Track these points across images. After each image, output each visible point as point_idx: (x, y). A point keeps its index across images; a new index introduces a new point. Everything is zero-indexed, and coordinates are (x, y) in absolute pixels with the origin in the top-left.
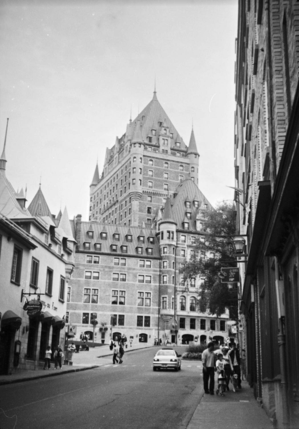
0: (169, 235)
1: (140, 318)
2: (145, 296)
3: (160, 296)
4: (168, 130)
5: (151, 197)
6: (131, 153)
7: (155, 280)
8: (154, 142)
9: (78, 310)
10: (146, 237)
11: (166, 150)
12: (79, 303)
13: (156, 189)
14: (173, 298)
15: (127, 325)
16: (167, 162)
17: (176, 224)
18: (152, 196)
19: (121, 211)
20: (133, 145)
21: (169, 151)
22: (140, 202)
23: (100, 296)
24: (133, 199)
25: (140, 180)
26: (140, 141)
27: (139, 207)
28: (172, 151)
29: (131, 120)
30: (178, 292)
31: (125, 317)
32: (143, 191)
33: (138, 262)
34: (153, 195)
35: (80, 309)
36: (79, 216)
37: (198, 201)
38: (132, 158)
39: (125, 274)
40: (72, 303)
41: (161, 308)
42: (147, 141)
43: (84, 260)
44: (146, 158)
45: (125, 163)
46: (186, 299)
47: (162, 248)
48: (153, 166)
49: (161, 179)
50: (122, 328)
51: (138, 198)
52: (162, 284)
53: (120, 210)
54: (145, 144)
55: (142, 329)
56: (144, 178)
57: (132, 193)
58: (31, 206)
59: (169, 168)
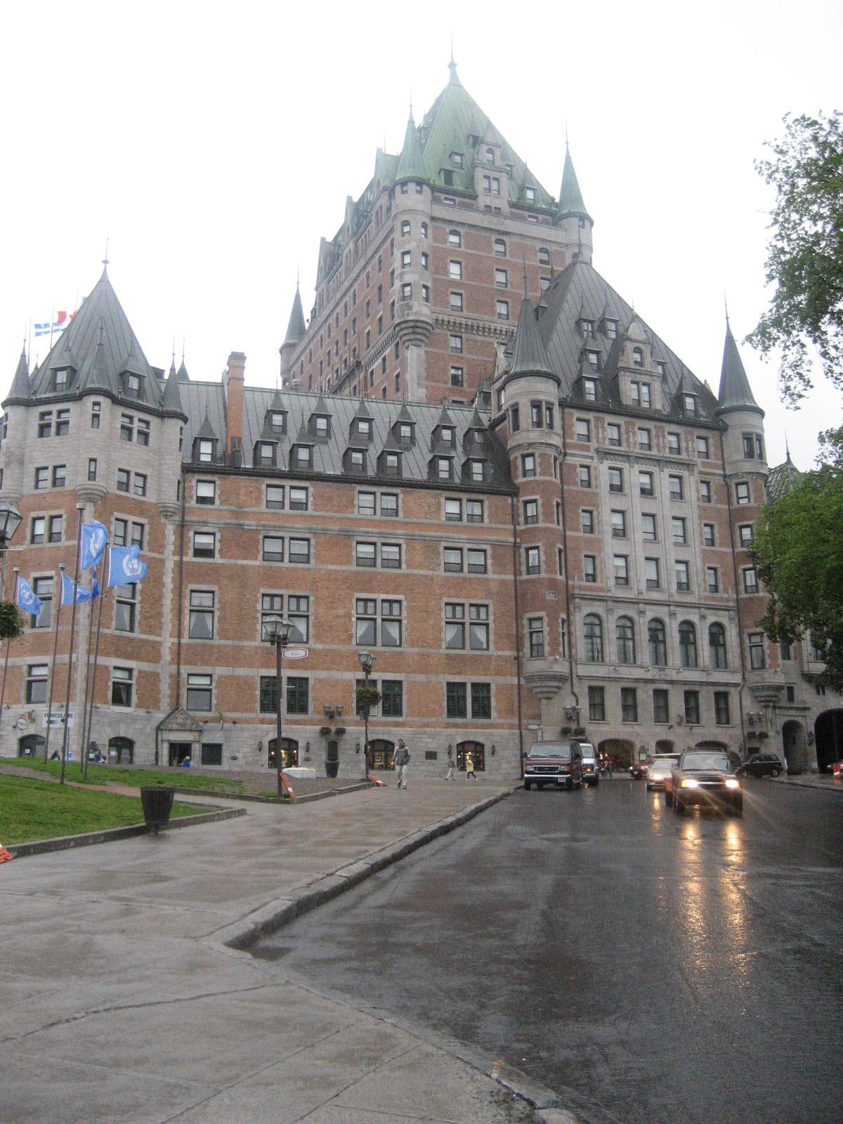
0: (539, 414)
1: (455, 690)
2: (470, 615)
3: (518, 617)
4: (498, 152)
5: (461, 337)
6: (393, 212)
8: (458, 185)
9: (241, 667)
10: (460, 434)
11: (495, 208)
12: (246, 643)
13: (475, 316)
14: (563, 621)
15: (411, 714)
16: (501, 237)
17: (559, 385)
18: (463, 335)
19: (369, 390)
20: (398, 189)
21: (506, 209)
22: (426, 352)
23: (316, 618)
24: (406, 344)
25: (425, 287)
26: (420, 174)
28: (514, 210)
30: (577, 601)
31: (405, 685)
32: (437, 320)
33: (439, 504)
34: (466, 332)
35: (251, 665)
36: (237, 360)
39: (399, 546)
40: (223, 642)
41: (523, 657)
42: (440, 182)
43: (259, 499)
44: (440, 225)
45: (376, 252)
46: (605, 625)
47: (516, 458)
48: (463, 249)
50: (397, 724)
51: (422, 341)
52: (525, 577)
53: (366, 389)
54: (434, 189)
55: (465, 726)
56: (435, 280)
57: (403, 326)
59: (508, 255)
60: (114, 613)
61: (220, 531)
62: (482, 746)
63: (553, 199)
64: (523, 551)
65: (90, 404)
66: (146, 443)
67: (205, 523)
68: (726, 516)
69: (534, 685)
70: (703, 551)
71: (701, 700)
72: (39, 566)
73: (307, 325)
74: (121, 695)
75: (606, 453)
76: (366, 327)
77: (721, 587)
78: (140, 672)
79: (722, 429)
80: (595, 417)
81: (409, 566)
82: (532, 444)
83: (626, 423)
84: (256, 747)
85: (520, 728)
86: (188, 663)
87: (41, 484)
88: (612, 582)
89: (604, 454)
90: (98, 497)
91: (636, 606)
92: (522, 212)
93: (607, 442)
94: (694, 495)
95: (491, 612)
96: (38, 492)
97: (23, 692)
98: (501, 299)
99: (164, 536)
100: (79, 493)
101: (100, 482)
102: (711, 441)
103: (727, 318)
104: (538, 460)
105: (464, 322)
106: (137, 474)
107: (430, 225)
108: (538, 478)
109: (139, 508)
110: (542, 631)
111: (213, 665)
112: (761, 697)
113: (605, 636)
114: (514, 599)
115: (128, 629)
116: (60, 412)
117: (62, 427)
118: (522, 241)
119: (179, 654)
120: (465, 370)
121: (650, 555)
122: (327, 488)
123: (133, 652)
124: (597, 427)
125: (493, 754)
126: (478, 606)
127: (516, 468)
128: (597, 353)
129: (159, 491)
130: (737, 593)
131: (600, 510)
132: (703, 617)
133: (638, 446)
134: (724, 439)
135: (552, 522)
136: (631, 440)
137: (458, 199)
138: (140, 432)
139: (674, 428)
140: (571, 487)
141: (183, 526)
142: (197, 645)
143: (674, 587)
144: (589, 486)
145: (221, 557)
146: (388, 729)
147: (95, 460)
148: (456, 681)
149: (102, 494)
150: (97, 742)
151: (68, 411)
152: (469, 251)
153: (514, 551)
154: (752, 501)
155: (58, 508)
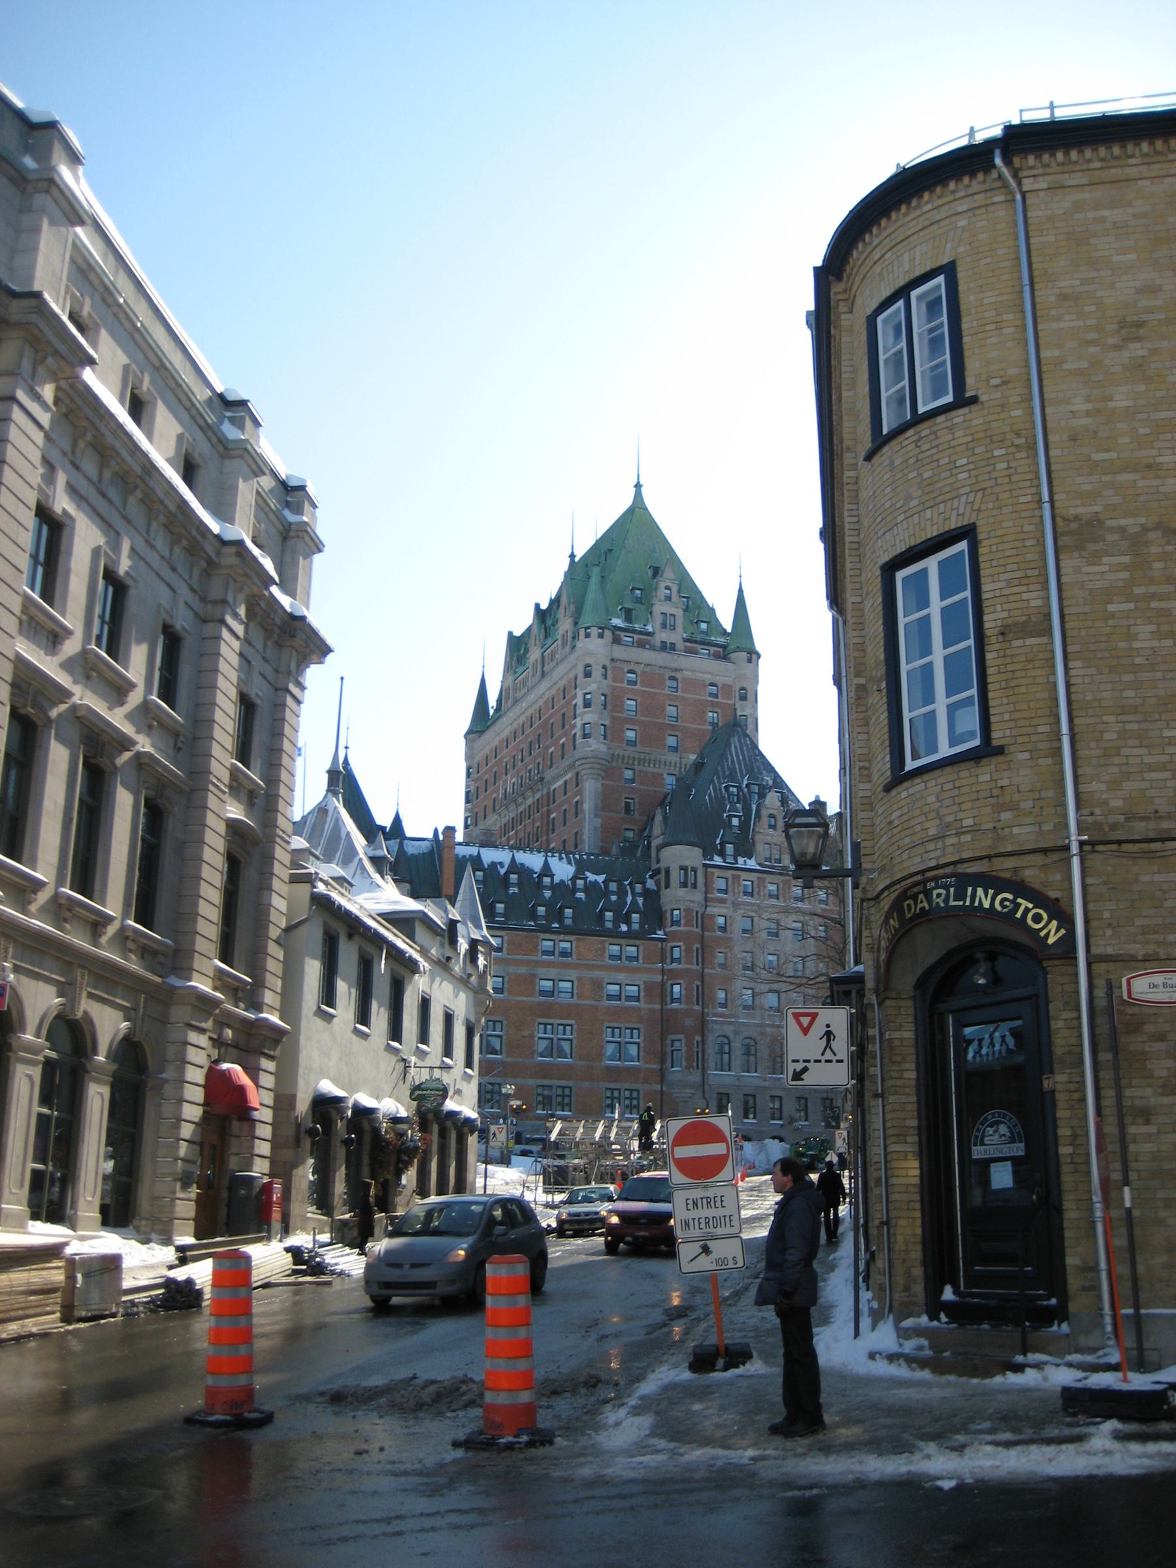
3: (663, 1039)
6: (578, 652)
13: (647, 750)
19: (552, 806)
29: (572, 556)
44: (618, 664)
45: (561, 679)
52: (670, 1006)
56: (613, 718)
73: (491, 712)
76: (548, 747)
81: (579, 998)
105: (637, 755)
108: (681, 928)
113: (733, 1053)
124: (733, 883)
137: (636, 637)
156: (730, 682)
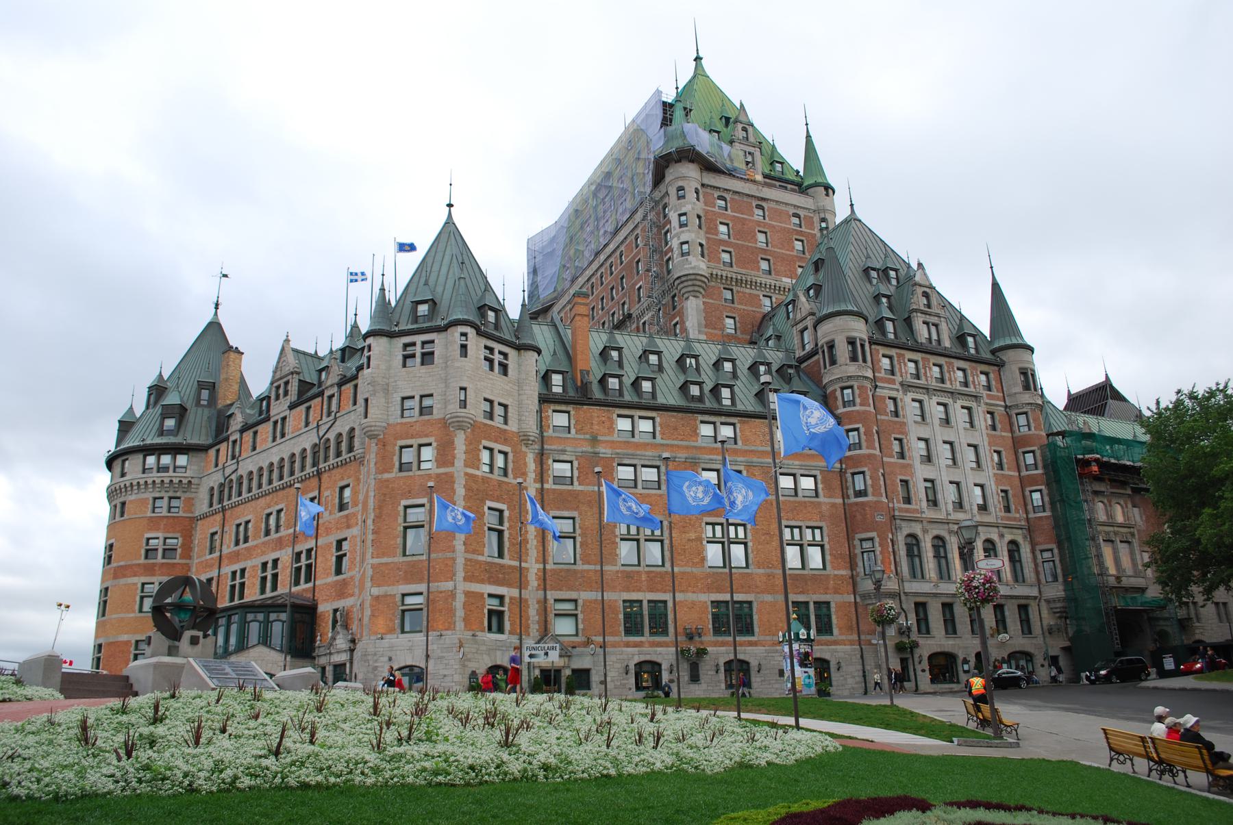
0: (854, 351)
3: (849, 539)
4: (750, 129)
5: (732, 290)
7: (828, 487)
13: (743, 271)
16: (760, 203)
17: (867, 321)
18: (734, 288)
21: (759, 178)
24: (686, 296)
25: (701, 245)
27: (704, 315)
30: (898, 521)
31: (755, 606)
32: (712, 274)
34: (737, 285)
37: (896, 270)
38: (672, 191)
40: (586, 567)
41: (857, 576)
44: (709, 190)
46: (922, 544)
47: (835, 390)
48: (729, 212)
49: (750, 244)
50: (751, 644)
52: (853, 500)
56: (708, 239)
57: (683, 279)
58: (429, 261)
59: (767, 218)
60: (486, 540)
61: (577, 459)
62: (826, 662)
63: (798, 172)
64: (849, 476)
65: (457, 335)
66: (505, 373)
67: (564, 451)
68: (1010, 442)
69: (870, 602)
70: (995, 474)
71: (1007, 613)
72: (409, 494)
74: (496, 620)
75: (909, 386)
77: (1013, 507)
78: (511, 598)
79: (1000, 365)
80: (897, 353)
82: (851, 377)
83: (922, 358)
84: (623, 671)
85: (860, 645)
86: (553, 589)
87: (406, 413)
88: (924, 504)
89: (906, 387)
90: (469, 426)
91: (946, 526)
92: (774, 182)
93: (909, 376)
94: (983, 427)
95: (825, 534)
96: (404, 420)
97: (398, 621)
98: (764, 256)
99: (525, 464)
100: (449, 421)
101: (470, 409)
102: (991, 376)
103: (991, 267)
104: (857, 392)
106: (500, 404)
107: (701, 191)
108: (857, 408)
109: (503, 437)
110: (874, 551)
111: (578, 590)
112: (1056, 608)
113: (924, 555)
114: (844, 521)
115: (496, 555)
116: (424, 343)
117: (426, 357)
118: (778, 207)
119: (545, 580)
120: (737, 319)
121: (952, 479)
122: (673, 418)
123: (504, 578)
125: (838, 669)
126: (813, 528)
127: (836, 398)
128: (888, 297)
129: (519, 420)
130: (1027, 512)
131: (908, 437)
132: (1002, 536)
133: (934, 380)
134: (1002, 374)
135: (875, 449)
136: (928, 375)
138: (500, 364)
139: (962, 364)
140: (883, 417)
141: (542, 455)
142: (561, 570)
143: (975, 508)
144: (897, 416)
145: (579, 485)
146: (743, 648)
147: (464, 389)
148: (800, 600)
149: (472, 422)
150: (477, 671)
151: (432, 342)
152: (736, 214)
153: (840, 476)
154: (1033, 429)
155: (427, 436)
156: (812, 215)
